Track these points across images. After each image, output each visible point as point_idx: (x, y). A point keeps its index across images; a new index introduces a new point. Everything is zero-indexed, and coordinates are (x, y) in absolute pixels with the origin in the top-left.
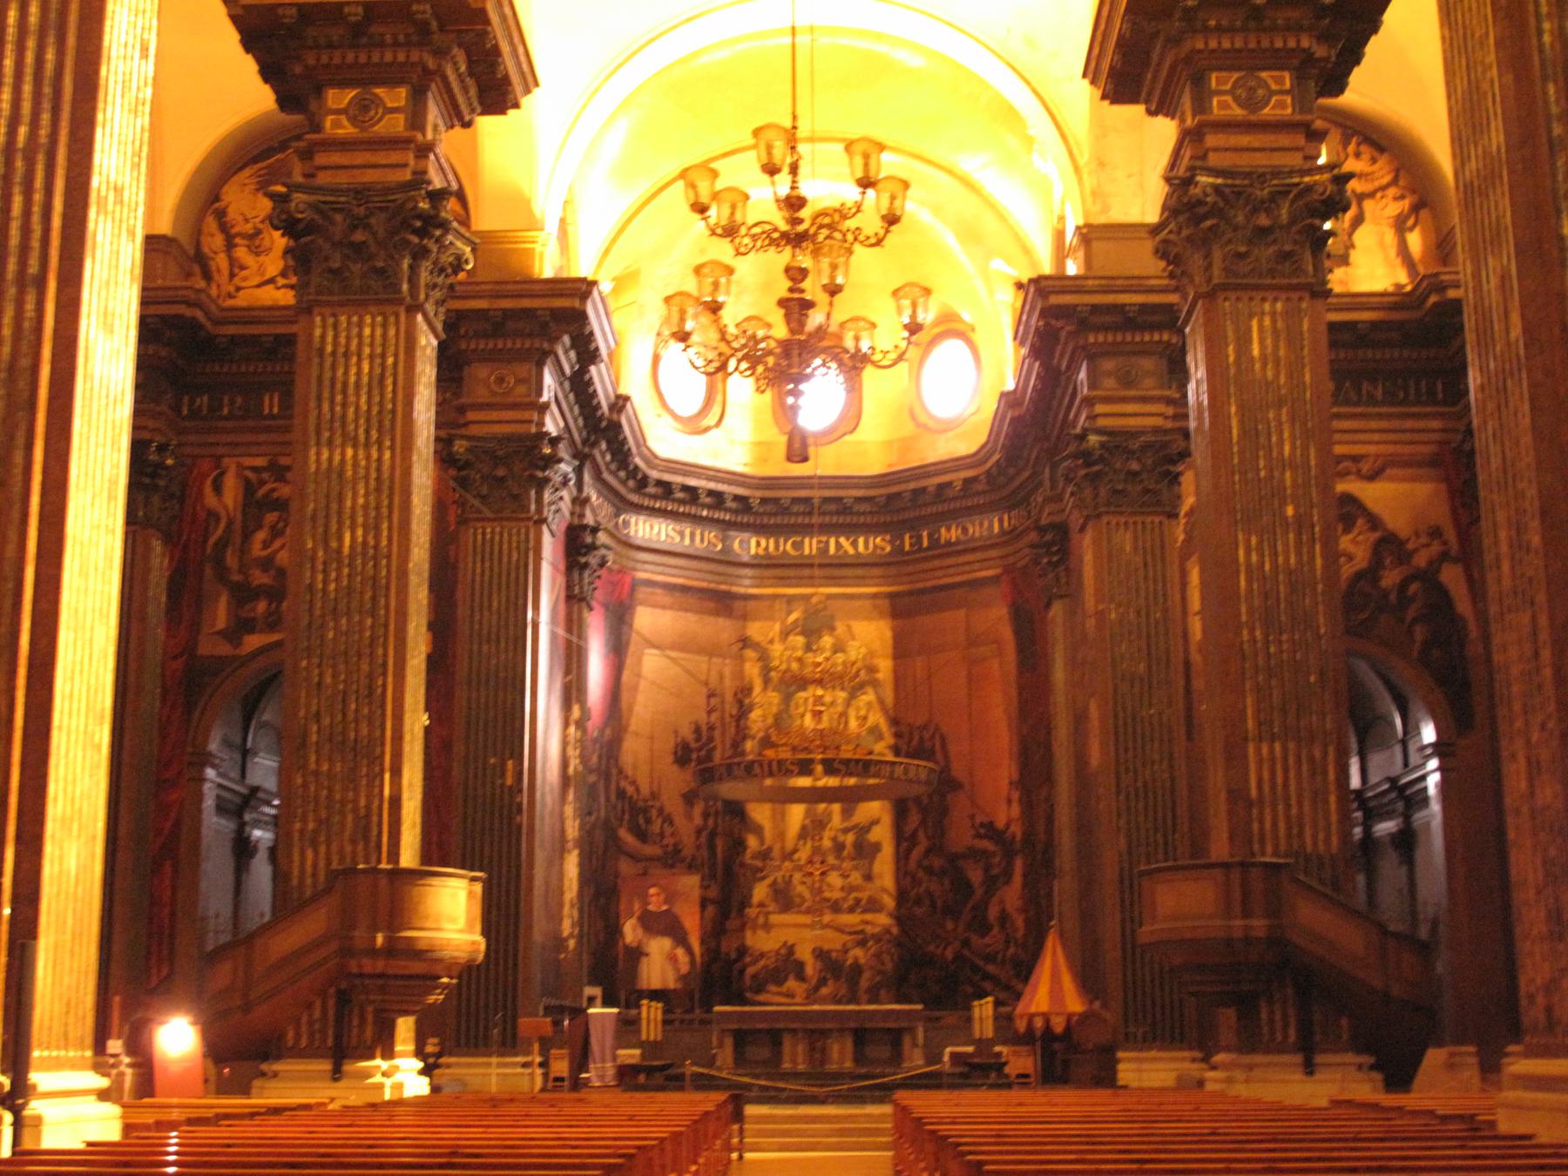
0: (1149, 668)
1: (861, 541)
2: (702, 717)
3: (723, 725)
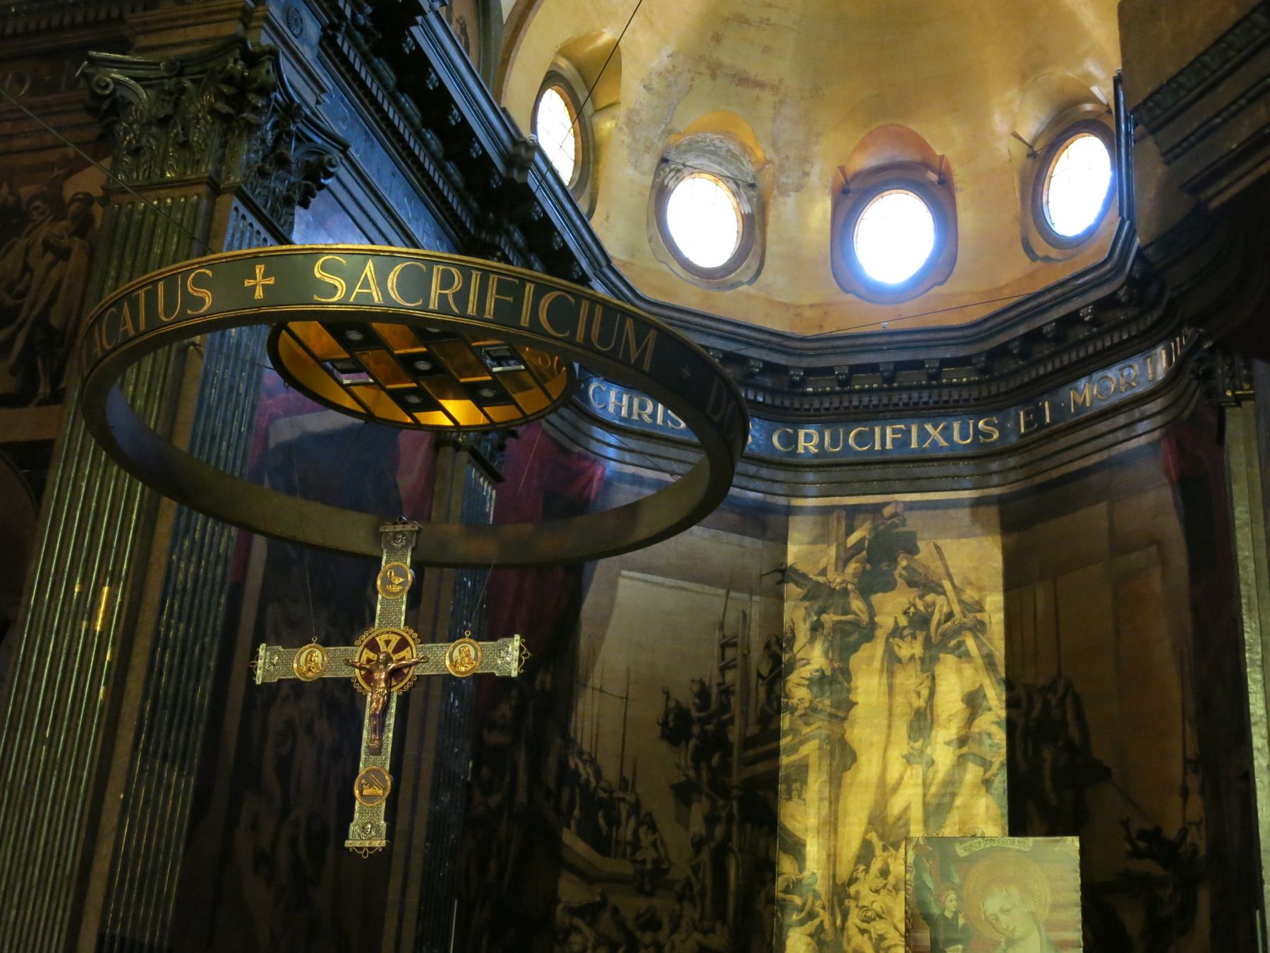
3: (746, 691)
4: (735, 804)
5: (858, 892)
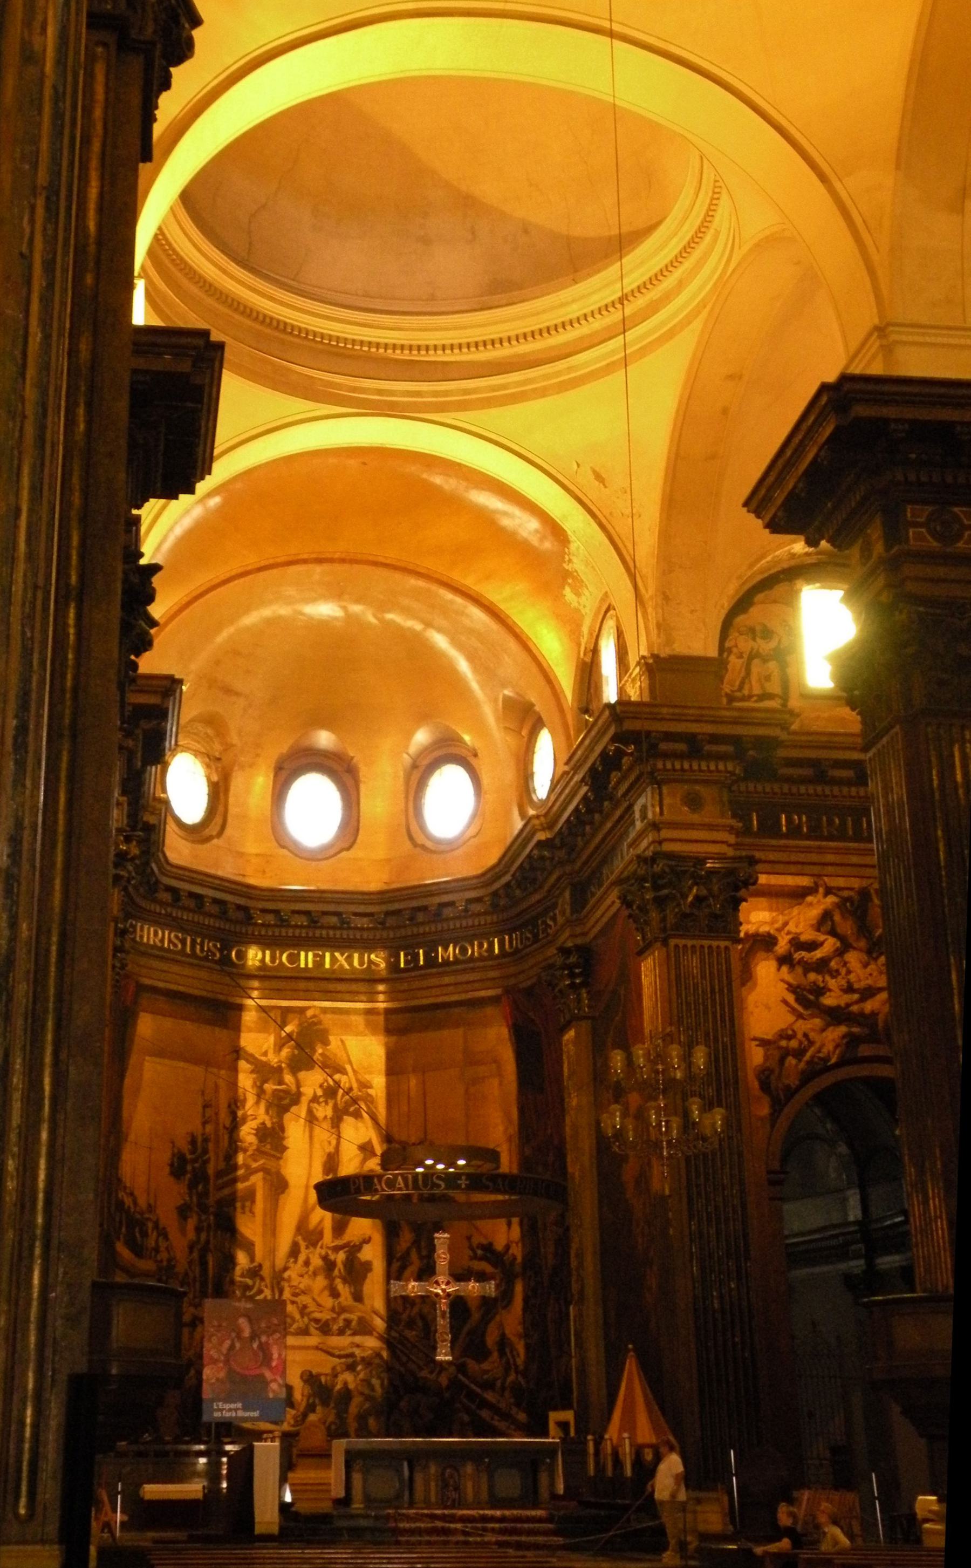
0: (718, 1090)
1: (356, 956)
2: (198, 1131)
4: (212, 1218)
5: (290, 1277)
